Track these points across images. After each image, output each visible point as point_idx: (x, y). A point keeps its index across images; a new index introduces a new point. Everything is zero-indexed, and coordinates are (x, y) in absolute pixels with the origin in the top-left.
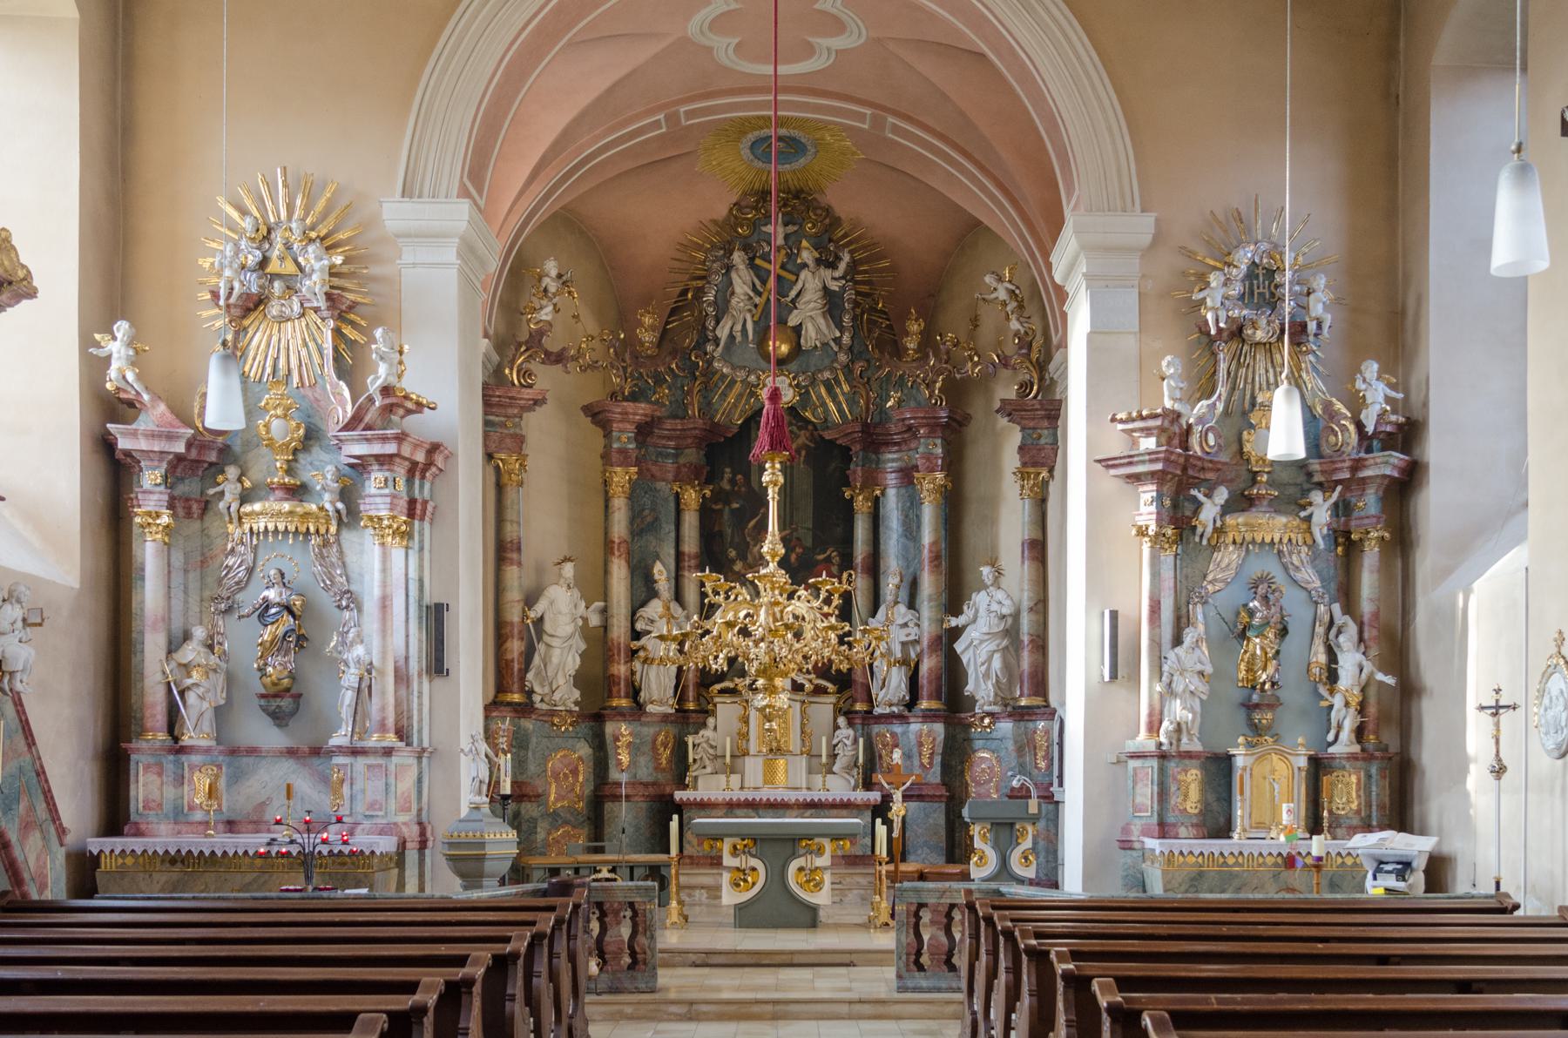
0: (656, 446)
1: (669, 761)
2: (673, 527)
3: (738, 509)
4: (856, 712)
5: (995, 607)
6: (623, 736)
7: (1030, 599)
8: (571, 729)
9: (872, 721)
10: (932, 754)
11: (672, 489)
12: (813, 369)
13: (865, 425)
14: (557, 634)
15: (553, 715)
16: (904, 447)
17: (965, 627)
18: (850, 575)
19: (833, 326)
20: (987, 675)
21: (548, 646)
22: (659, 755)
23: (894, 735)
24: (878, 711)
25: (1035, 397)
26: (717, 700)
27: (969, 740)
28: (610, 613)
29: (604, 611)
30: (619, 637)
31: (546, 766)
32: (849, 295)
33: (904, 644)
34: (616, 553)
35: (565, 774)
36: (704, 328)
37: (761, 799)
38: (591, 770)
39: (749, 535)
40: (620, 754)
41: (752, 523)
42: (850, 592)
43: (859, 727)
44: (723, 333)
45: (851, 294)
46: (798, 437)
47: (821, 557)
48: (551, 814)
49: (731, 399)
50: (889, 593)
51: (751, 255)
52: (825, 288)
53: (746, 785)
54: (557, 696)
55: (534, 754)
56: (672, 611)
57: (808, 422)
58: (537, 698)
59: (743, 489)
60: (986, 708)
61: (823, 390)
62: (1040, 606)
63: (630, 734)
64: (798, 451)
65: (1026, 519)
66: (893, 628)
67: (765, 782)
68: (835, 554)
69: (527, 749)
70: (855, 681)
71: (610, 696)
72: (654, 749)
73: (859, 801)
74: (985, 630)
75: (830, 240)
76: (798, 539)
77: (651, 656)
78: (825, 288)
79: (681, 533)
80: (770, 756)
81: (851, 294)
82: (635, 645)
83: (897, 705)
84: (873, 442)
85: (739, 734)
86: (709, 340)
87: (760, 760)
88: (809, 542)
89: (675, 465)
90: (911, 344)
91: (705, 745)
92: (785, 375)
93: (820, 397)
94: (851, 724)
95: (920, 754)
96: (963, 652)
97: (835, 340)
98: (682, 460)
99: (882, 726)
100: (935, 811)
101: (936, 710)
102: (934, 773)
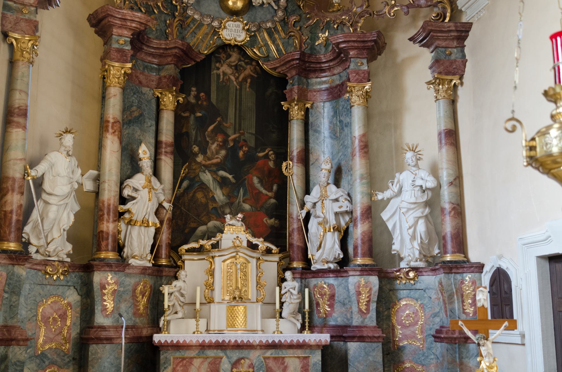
0: (143, 61)
1: (146, 308)
2: (154, 123)
3: (200, 117)
5: (419, 182)
6: (109, 284)
7: (449, 175)
8: (62, 277)
10: (368, 302)
11: (154, 94)
12: (259, 21)
13: (303, 54)
14: (55, 193)
15: (47, 265)
17: (389, 200)
20: (413, 237)
21: (46, 203)
22: (138, 302)
25: (450, 20)
26: (185, 257)
27: (393, 290)
28: (101, 180)
29: (97, 179)
30: (109, 200)
31: (37, 311)
33: (336, 214)
35: (54, 319)
37: (230, 341)
38: (78, 315)
39: (209, 136)
40: (105, 301)
41: (211, 128)
46: (245, 69)
47: (261, 154)
48: (39, 355)
49: (200, 35)
54: (51, 248)
55: (26, 300)
56: (153, 183)
57: (252, 59)
58: (32, 249)
60: (413, 264)
61: (266, 35)
62: (457, 181)
63: (115, 283)
64: (245, 79)
65: (442, 114)
66: (327, 203)
67: (228, 326)
68: (271, 152)
69: (19, 294)
71: (99, 249)
72: (134, 296)
73: (312, 342)
74: (413, 200)
76: (245, 141)
77: (134, 218)
79: (160, 128)
80: (233, 303)
82: (122, 208)
83: (332, 262)
84: (305, 70)
87: (224, 307)
88: (252, 143)
92: (239, 21)
93: (264, 40)
95: (358, 302)
96: (388, 220)
98: (163, 74)
99: (320, 279)
100: (374, 350)
101: (371, 265)
102: (370, 317)
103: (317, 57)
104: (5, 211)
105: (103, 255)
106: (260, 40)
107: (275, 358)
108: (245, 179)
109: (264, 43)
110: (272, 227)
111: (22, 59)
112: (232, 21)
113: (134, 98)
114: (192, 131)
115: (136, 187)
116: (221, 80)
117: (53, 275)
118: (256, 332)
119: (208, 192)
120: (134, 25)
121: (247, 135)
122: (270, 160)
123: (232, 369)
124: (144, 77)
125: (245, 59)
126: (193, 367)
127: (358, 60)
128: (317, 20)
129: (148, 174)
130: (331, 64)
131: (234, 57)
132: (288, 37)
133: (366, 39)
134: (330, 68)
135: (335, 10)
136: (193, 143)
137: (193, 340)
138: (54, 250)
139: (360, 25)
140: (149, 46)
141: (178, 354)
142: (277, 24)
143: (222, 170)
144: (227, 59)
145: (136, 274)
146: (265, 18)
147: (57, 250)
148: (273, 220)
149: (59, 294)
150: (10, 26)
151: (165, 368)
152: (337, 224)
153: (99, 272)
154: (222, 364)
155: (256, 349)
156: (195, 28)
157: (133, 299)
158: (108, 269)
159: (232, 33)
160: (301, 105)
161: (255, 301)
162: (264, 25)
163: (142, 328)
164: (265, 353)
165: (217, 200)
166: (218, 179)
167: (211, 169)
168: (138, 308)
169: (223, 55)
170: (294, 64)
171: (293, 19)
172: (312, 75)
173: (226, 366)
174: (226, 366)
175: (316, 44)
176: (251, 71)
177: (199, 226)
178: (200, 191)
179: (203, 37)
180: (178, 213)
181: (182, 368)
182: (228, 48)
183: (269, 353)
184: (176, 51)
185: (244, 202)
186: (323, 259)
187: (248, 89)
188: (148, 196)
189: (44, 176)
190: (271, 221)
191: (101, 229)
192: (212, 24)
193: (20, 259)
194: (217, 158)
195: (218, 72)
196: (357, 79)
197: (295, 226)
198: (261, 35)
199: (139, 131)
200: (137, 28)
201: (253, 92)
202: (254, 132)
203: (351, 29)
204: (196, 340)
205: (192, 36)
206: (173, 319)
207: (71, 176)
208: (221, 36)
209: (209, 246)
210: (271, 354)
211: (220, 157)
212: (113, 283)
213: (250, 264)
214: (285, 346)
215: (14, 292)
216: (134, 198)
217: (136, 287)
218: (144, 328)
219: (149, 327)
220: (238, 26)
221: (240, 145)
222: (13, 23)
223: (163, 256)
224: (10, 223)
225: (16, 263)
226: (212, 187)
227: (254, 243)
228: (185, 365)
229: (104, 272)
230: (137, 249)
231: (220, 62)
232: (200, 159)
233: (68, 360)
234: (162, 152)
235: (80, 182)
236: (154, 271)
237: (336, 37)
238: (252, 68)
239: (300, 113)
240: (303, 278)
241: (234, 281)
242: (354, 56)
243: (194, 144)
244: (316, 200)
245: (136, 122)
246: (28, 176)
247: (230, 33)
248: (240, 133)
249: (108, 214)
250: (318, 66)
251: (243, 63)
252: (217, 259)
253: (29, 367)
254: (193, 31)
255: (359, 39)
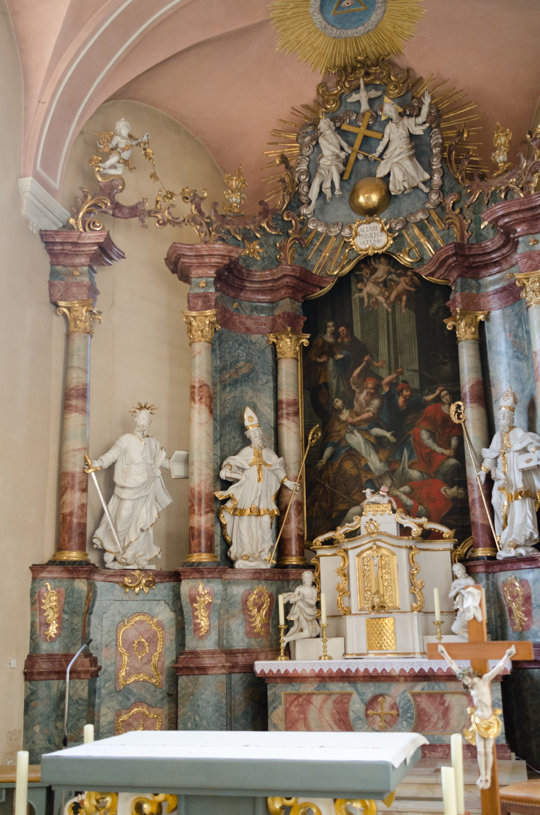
2: (271, 378)
3: (341, 359)
4: (478, 559)
6: (200, 595)
8: (146, 590)
9: (497, 568)
11: (268, 341)
12: (405, 214)
15: (125, 576)
16: (505, 266)
18: (459, 407)
19: (421, 168)
21: (121, 499)
22: (252, 617)
23: (523, 583)
24: (501, 555)
26: (319, 552)
29: (187, 461)
32: (436, 139)
33: (525, 472)
34: (197, 398)
35: (140, 643)
36: (298, 193)
38: (173, 637)
39: (354, 384)
42: (460, 424)
43: (483, 576)
44: (314, 194)
45: (437, 139)
46: (397, 284)
47: (430, 397)
50: (501, 417)
51: (338, 125)
52: (412, 137)
53: (349, 651)
54: (129, 554)
56: (265, 458)
57: (405, 268)
58: (108, 558)
59: (346, 340)
61: (416, 231)
64: (398, 298)
67: (370, 647)
68: (445, 392)
70: (474, 523)
75: (413, 98)
76: (405, 382)
78: (412, 137)
79: (279, 383)
80: (373, 615)
81: (437, 139)
82: (220, 495)
83: (525, 546)
84: (470, 267)
85: (338, 588)
86: (303, 204)
87: (362, 620)
88: (416, 384)
89: (271, 317)
90: (500, 157)
91: (300, 604)
93: (414, 238)
94: (470, 572)
97: (425, 183)
98: (277, 312)
99: (509, 573)
103: (483, 245)
104: (63, 514)
105: (195, 558)
106: (409, 240)
107: (430, 695)
108: (409, 436)
109: (415, 242)
110: (454, 499)
111: (76, 330)
112: (365, 223)
113: (240, 351)
114: (332, 380)
115: (240, 466)
116: (366, 305)
117: (135, 587)
118: (413, 656)
119: (360, 460)
120: (214, 260)
121: (407, 375)
122: (444, 404)
123: (367, 710)
124: (253, 321)
125: (397, 270)
126: (312, 707)
127: (530, 238)
128: (481, 193)
129: (256, 446)
130: (505, 251)
131: (382, 270)
132: (447, 227)
133: (534, 205)
134: (506, 257)
135: (500, 172)
136: (334, 396)
137: (306, 668)
138: (134, 556)
139: (533, 185)
140: (253, 281)
141: (290, 689)
142: (432, 212)
143: (377, 427)
144: (372, 275)
145: (245, 579)
146: (414, 208)
147: (137, 555)
148: (454, 489)
149: (145, 611)
150: (59, 295)
151: (275, 708)
152: (525, 487)
153: (186, 581)
154: (351, 703)
155: (398, 681)
156: (321, 244)
157: (244, 614)
158: (197, 576)
159: (368, 239)
160: (468, 319)
161: (409, 609)
162: (412, 218)
163: (258, 653)
164: (412, 687)
165: (372, 469)
166: (372, 439)
167: (361, 427)
168: (253, 625)
169: (366, 272)
170: (451, 264)
171: (450, 202)
172: (483, 273)
173: (357, 706)
174: (357, 706)
175: (482, 227)
176: (407, 284)
177: (350, 507)
178: (348, 460)
179: (331, 254)
180: (321, 492)
181: (297, 709)
182: (372, 260)
183: (419, 687)
184: (287, 279)
185: (410, 467)
186: (511, 542)
187: (404, 310)
188: (257, 475)
189: (116, 466)
190: (453, 491)
191: (191, 525)
192: (342, 233)
193: (80, 571)
194: (368, 411)
195: (361, 295)
196: (530, 266)
197: (476, 496)
198: (409, 232)
199: (251, 392)
200: (218, 263)
201: (412, 313)
202: (417, 368)
203: (522, 195)
204: (310, 668)
205: (317, 256)
206: (298, 640)
207: (150, 461)
208: (354, 247)
209: (341, 535)
210: (423, 689)
211: (372, 409)
212: (205, 594)
213: (395, 557)
214: (442, 676)
215: (75, 612)
216: (238, 480)
217: (247, 597)
218: (263, 652)
219: (271, 651)
220: (375, 228)
221: (399, 388)
222: (62, 290)
223: (294, 552)
224: (70, 528)
225: (76, 576)
226: (364, 453)
227: (405, 526)
228: (302, 705)
229: (193, 580)
230: (248, 546)
231: (362, 281)
232: (345, 415)
233: (161, 696)
234: (283, 414)
235: (167, 466)
236: (274, 574)
237: (488, 212)
238: (407, 281)
239: (469, 331)
240: (490, 573)
241: (373, 583)
242: (522, 233)
243: (336, 397)
244: (495, 455)
245: (245, 381)
246: (89, 468)
247: (364, 240)
248: (397, 372)
249: (200, 506)
250: (488, 258)
251: (394, 277)
252: (350, 552)
253: (108, 705)
254: (318, 248)
255: (523, 208)
